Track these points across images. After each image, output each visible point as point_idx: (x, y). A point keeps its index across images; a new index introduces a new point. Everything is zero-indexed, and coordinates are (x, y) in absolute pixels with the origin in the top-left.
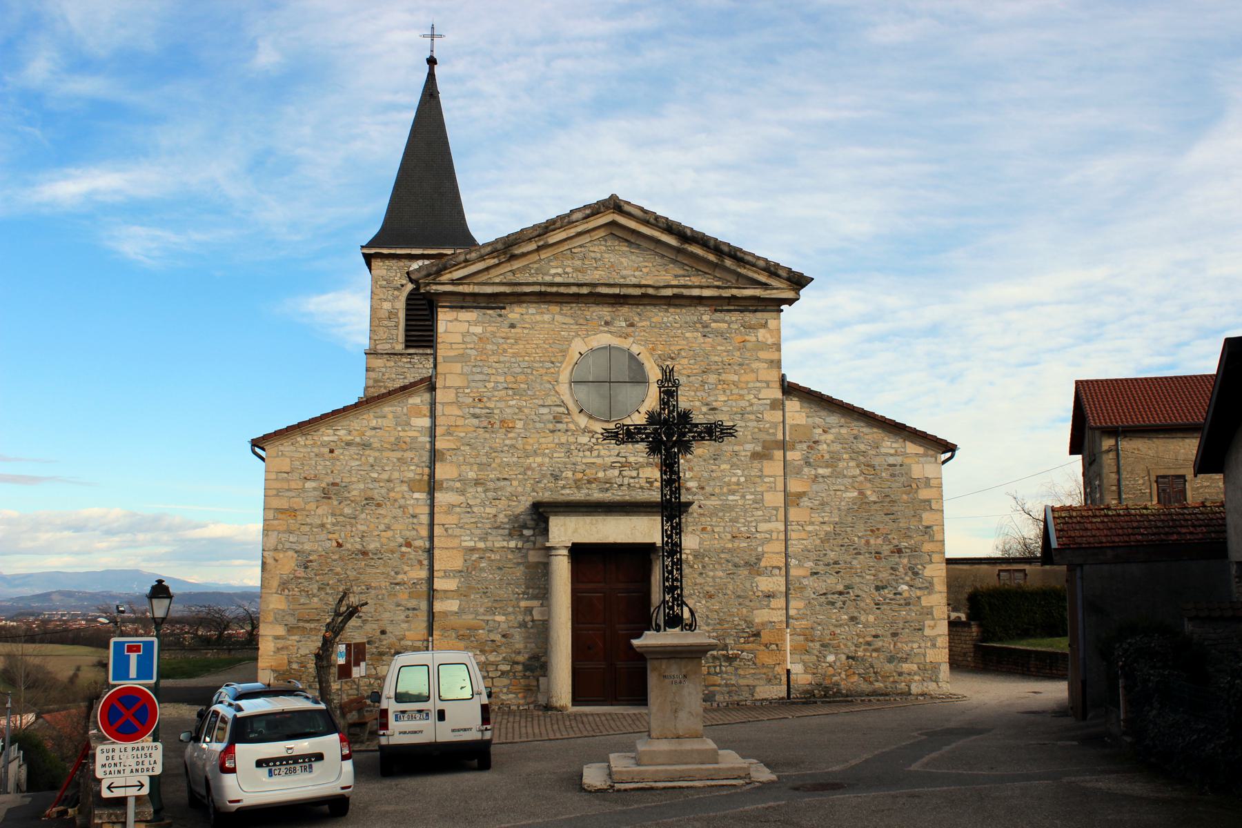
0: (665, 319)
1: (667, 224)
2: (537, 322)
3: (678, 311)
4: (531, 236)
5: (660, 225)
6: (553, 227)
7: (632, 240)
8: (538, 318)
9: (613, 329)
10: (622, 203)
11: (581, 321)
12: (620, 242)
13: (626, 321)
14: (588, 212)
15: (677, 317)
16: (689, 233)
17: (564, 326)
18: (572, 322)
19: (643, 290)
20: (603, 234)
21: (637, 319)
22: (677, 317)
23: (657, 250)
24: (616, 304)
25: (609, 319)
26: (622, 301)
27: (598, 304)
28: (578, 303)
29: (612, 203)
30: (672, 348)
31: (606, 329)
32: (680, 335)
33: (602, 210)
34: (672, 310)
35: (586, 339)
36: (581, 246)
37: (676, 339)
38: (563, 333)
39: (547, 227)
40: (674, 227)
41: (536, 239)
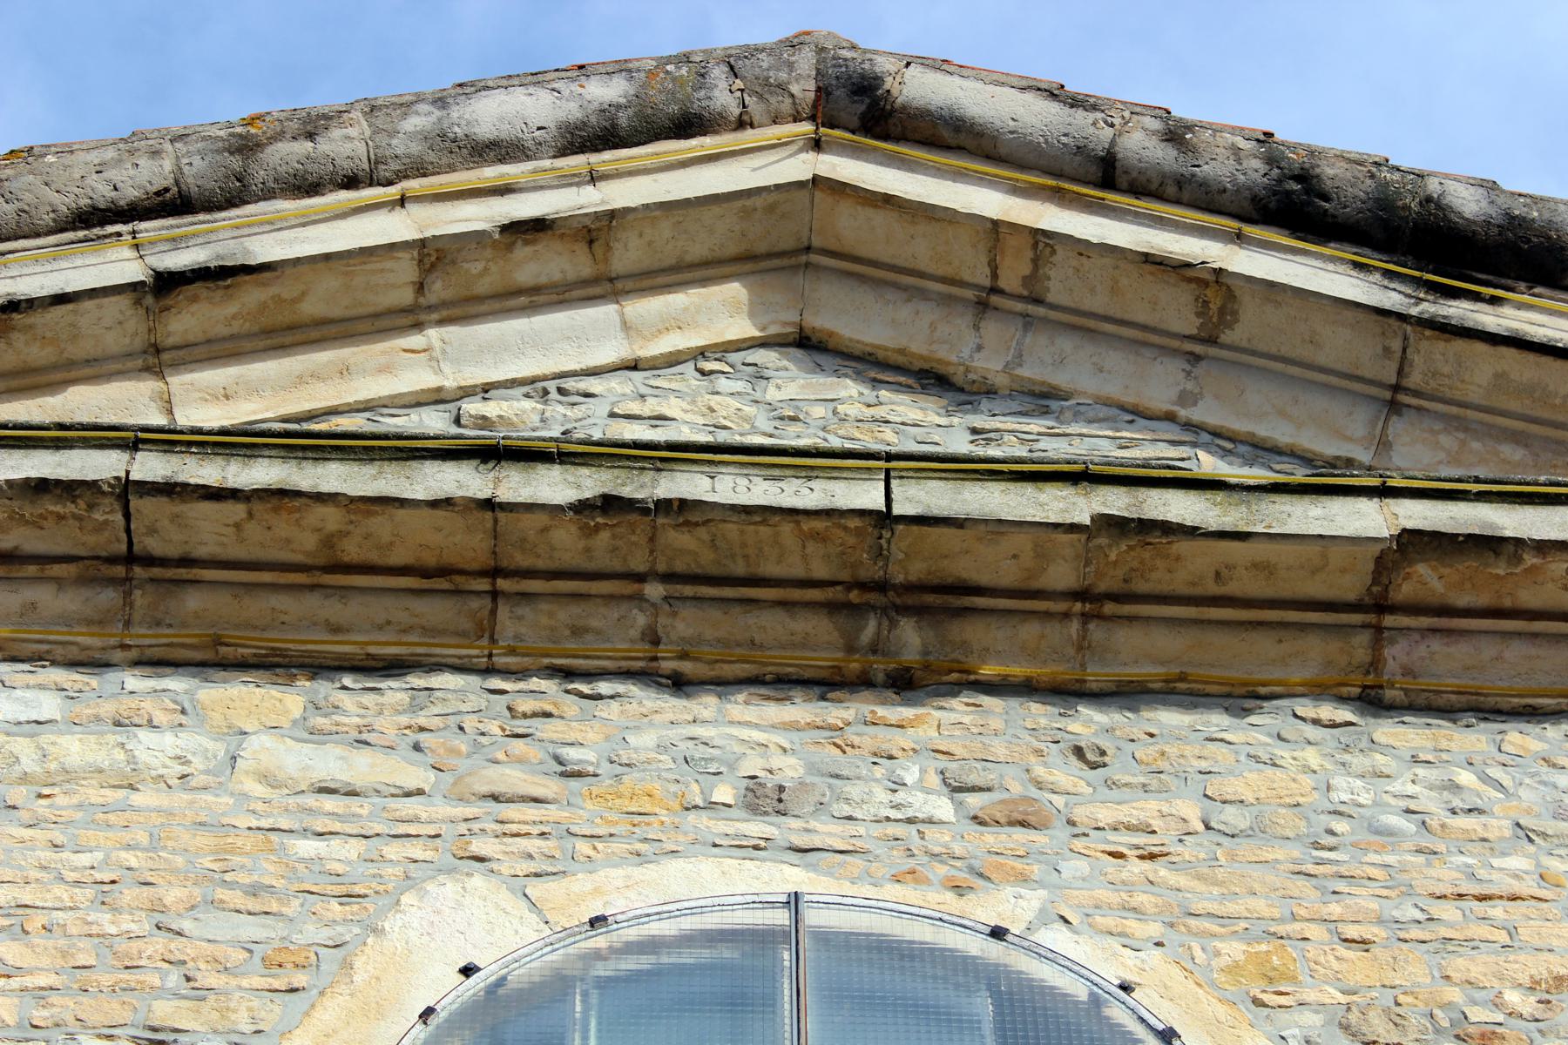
0: (1346, 788)
1: (1272, 160)
2: (69, 776)
3: (1473, 739)
4: (101, 192)
5: (1216, 168)
6: (288, 154)
7: (990, 364)
8: (74, 749)
9: (828, 832)
10: (884, 65)
11: (512, 779)
12: (876, 383)
13: (957, 789)
14: (606, 92)
15: (1466, 778)
16: (1468, 204)
17: (330, 803)
18: (415, 775)
19: (1115, 501)
20: (743, 328)
21: (1065, 774)
22: (1466, 778)
23: (1196, 414)
24: (860, 683)
25: (790, 769)
26: (911, 640)
27: (679, 684)
28: (489, 671)
29: (806, 61)
30: (1460, 965)
31: (756, 828)
32: (1529, 887)
33: (722, 96)
34: (1391, 732)
35: (536, 889)
36: (533, 386)
37: (1497, 911)
38: (307, 847)
39: (246, 146)
40: (1329, 171)
41: (148, 228)
